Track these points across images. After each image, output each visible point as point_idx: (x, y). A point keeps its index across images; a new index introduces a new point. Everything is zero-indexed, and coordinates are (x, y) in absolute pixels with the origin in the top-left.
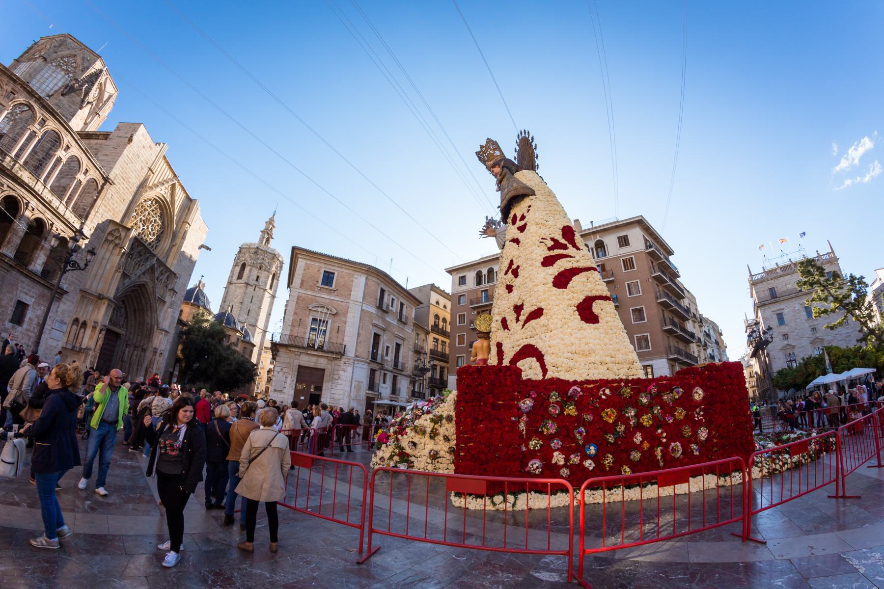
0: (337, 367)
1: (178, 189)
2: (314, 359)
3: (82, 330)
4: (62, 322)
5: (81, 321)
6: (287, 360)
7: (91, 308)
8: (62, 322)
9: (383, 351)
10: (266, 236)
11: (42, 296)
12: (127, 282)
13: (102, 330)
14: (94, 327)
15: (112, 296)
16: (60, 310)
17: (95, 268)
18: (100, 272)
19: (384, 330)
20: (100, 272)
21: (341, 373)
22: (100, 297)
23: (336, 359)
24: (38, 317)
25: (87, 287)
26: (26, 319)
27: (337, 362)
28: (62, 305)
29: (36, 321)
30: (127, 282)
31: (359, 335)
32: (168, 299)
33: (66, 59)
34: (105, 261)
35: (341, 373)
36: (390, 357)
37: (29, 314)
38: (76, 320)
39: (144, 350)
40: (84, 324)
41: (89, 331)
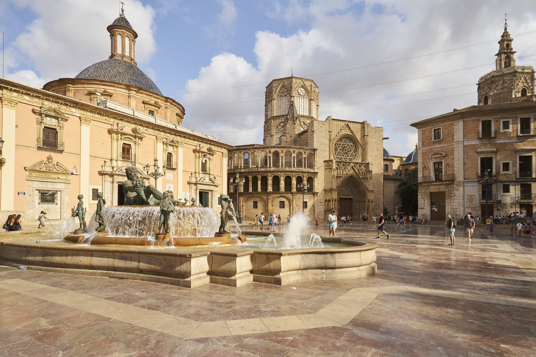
0: (452, 189)
1: (350, 124)
2: (437, 187)
4: (321, 202)
6: (424, 191)
8: (321, 202)
9: (498, 168)
10: (503, 56)
12: (341, 179)
19: (496, 152)
21: (456, 192)
23: (451, 184)
27: (452, 186)
30: (341, 179)
31: (465, 164)
32: (368, 176)
35: (456, 192)
36: (515, 169)
37: (308, 204)
39: (364, 202)
41: (331, 202)
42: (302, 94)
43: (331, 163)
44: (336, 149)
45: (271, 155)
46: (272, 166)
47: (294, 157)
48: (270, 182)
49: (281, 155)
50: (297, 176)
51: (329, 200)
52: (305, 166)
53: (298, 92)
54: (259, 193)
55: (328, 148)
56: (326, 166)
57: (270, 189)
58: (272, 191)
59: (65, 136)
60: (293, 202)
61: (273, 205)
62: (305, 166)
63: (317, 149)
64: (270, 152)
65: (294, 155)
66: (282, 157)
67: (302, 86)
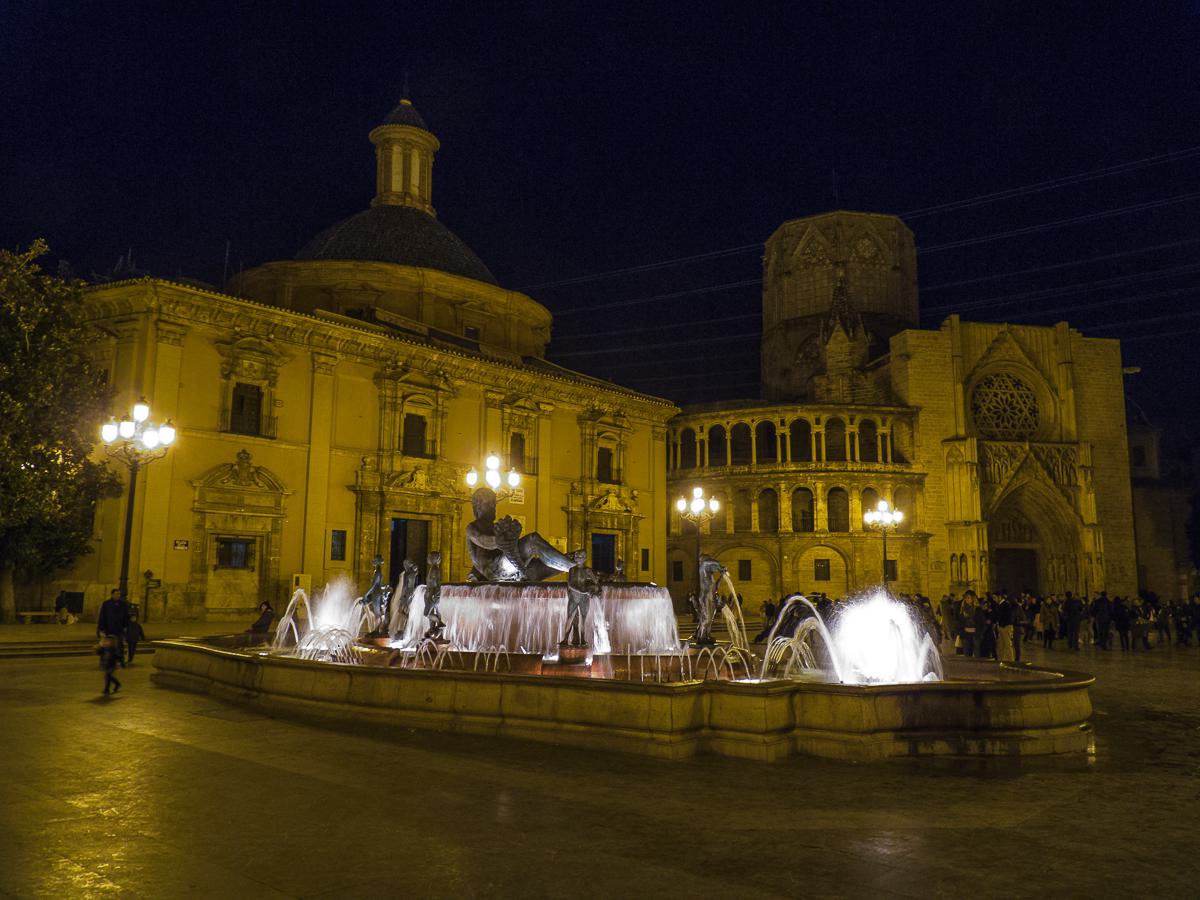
3: (964, 564)
5: (959, 554)
7: (964, 538)
11: (906, 547)
13: (981, 558)
14: (974, 557)
15: (979, 519)
16: (931, 553)
17: (951, 497)
18: (957, 499)
20: (957, 499)
22: (967, 524)
24: (910, 567)
25: (951, 519)
26: (899, 573)
28: (930, 547)
29: (909, 571)
33: (808, 251)
34: (957, 486)
37: (900, 568)
38: (954, 555)
40: (963, 557)
42: (867, 255)
43: (962, 450)
44: (976, 409)
45: (787, 431)
46: (789, 458)
47: (852, 436)
48: (785, 506)
49: (815, 429)
50: (862, 488)
51: (963, 557)
52: (885, 460)
53: (857, 252)
54: (754, 535)
55: (952, 404)
56: (950, 455)
57: (786, 522)
58: (791, 529)
59: (288, 399)
60: (853, 561)
61: (795, 573)
62: (885, 460)
63: (919, 408)
64: (783, 423)
65: (852, 428)
66: (818, 435)
67: (867, 235)
